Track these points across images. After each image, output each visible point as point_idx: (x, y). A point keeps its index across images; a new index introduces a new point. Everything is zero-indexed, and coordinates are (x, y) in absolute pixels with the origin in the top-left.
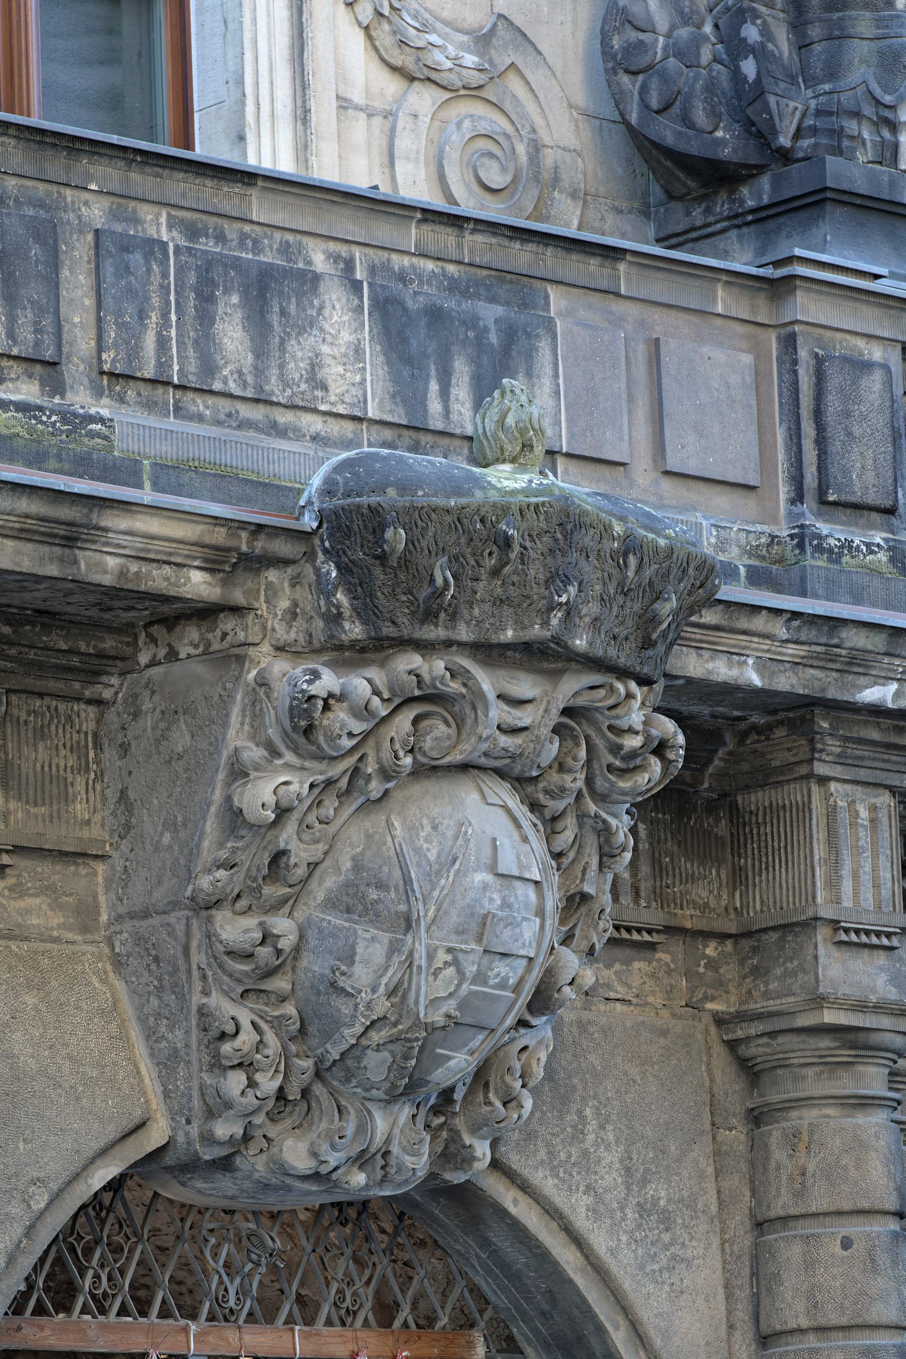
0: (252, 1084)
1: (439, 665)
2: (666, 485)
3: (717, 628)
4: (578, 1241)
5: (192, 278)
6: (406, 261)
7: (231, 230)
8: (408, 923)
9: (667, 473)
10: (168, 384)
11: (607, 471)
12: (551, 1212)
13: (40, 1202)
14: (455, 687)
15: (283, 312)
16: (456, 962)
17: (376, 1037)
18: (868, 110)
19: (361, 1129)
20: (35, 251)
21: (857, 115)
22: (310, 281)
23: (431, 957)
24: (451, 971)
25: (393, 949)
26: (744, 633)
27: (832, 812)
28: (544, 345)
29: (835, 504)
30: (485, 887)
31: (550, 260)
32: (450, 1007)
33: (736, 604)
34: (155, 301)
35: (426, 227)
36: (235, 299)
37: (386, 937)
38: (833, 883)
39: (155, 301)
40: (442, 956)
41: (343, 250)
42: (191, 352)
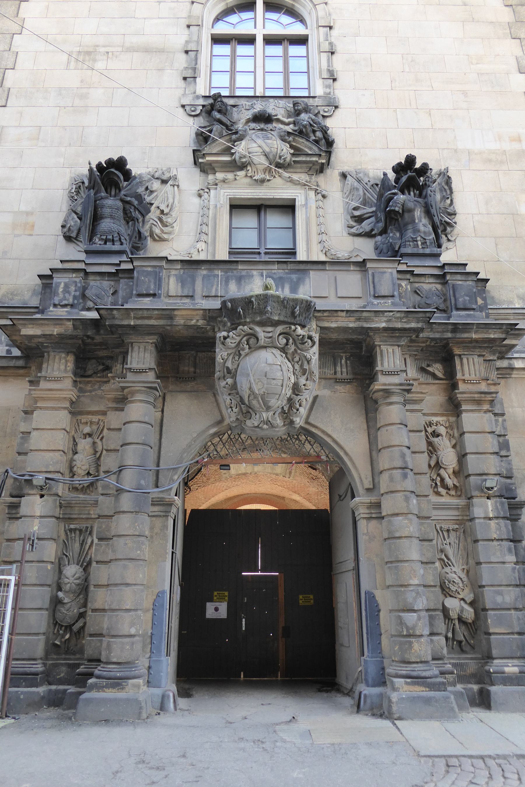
0: (232, 410)
1: (246, 327)
2: (339, 299)
3: (328, 316)
4: (329, 436)
5: (224, 279)
6: (276, 271)
7: (235, 272)
8: (248, 375)
9: (339, 297)
10: (218, 296)
11: (324, 299)
12: (323, 432)
13: (195, 435)
14: (251, 331)
15: (245, 282)
16: (261, 381)
17: (250, 398)
18: (411, 240)
19: (260, 417)
20: (189, 279)
21: (409, 241)
22: (253, 276)
23: (255, 381)
24: (260, 383)
25: (247, 380)
26: (337, 316)
27: (381, 351)
28: (307, 280)
29: (377, 297)
30: (265, 366)
31: (309, 267)
32: (264, 390)
33: (332, 310)
34: (215, 284)
35: (279, 265)
36: (234, 281)
37: (246, 378)
38: (382, 364)
39: (215, 284)
40: (257, 380)
41: (261, 271)
42: (223, 290)
